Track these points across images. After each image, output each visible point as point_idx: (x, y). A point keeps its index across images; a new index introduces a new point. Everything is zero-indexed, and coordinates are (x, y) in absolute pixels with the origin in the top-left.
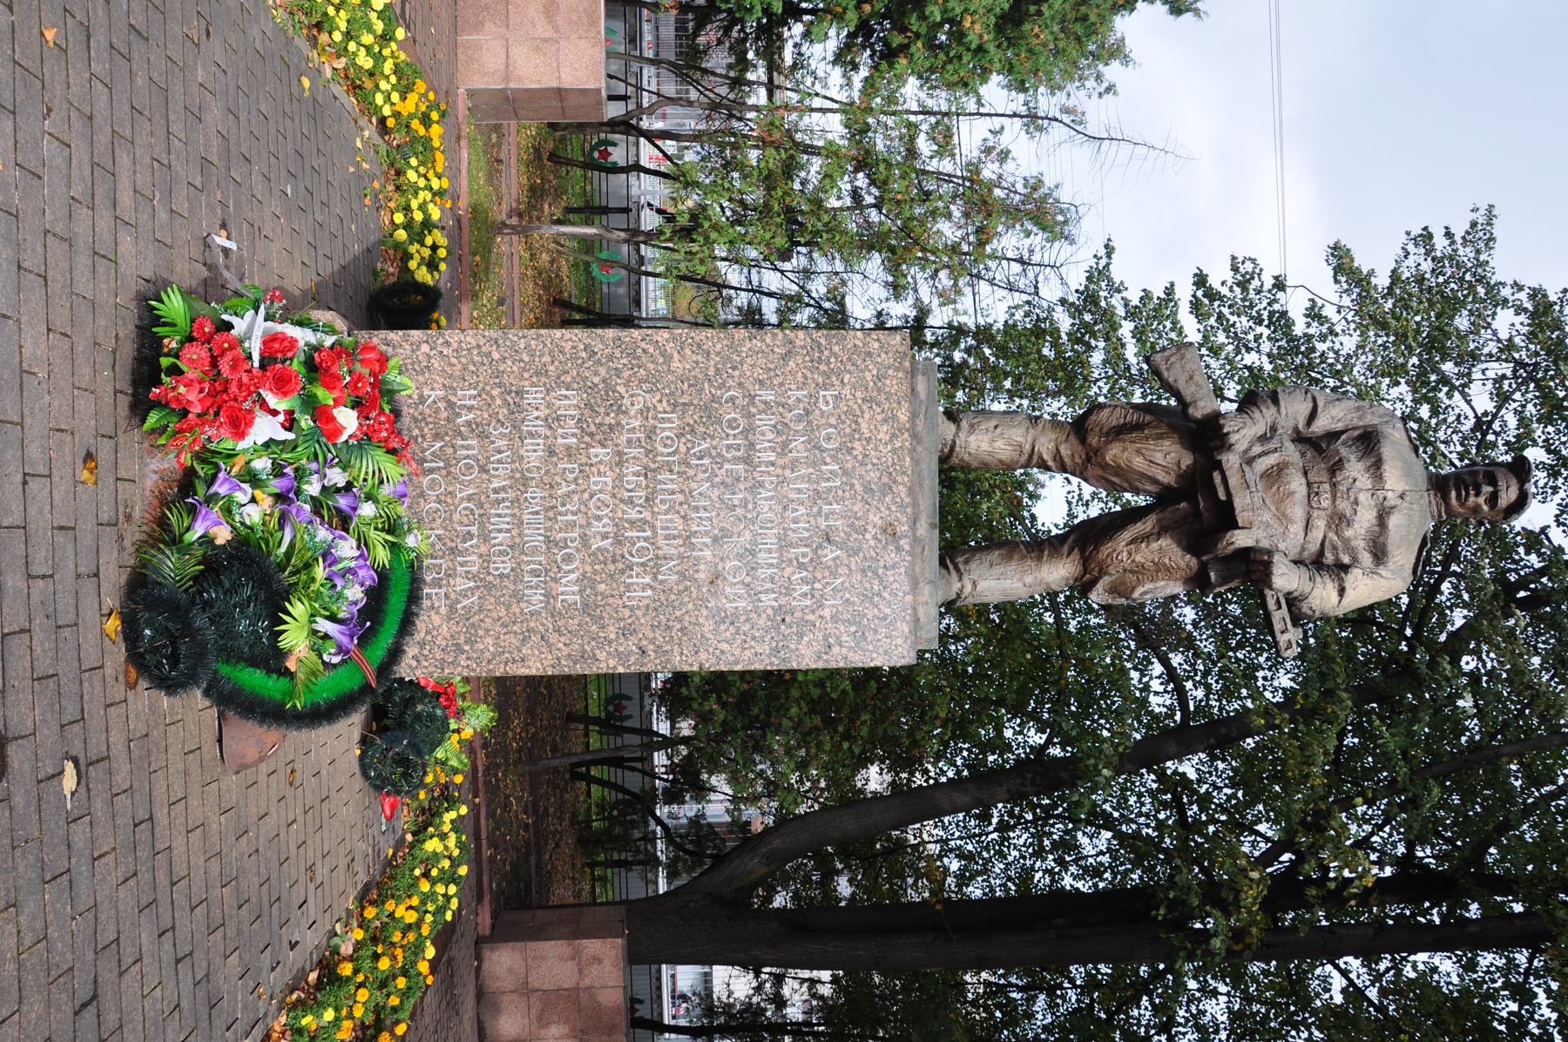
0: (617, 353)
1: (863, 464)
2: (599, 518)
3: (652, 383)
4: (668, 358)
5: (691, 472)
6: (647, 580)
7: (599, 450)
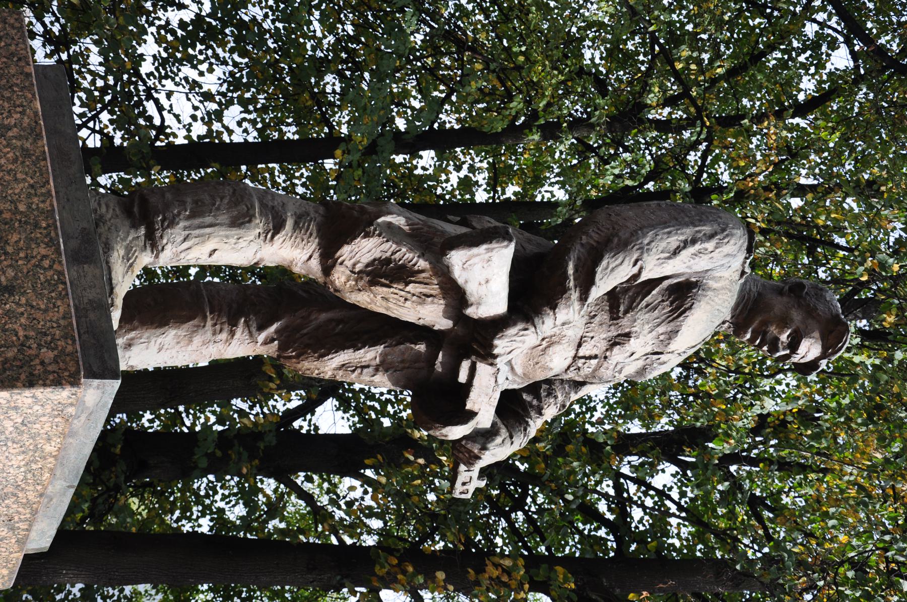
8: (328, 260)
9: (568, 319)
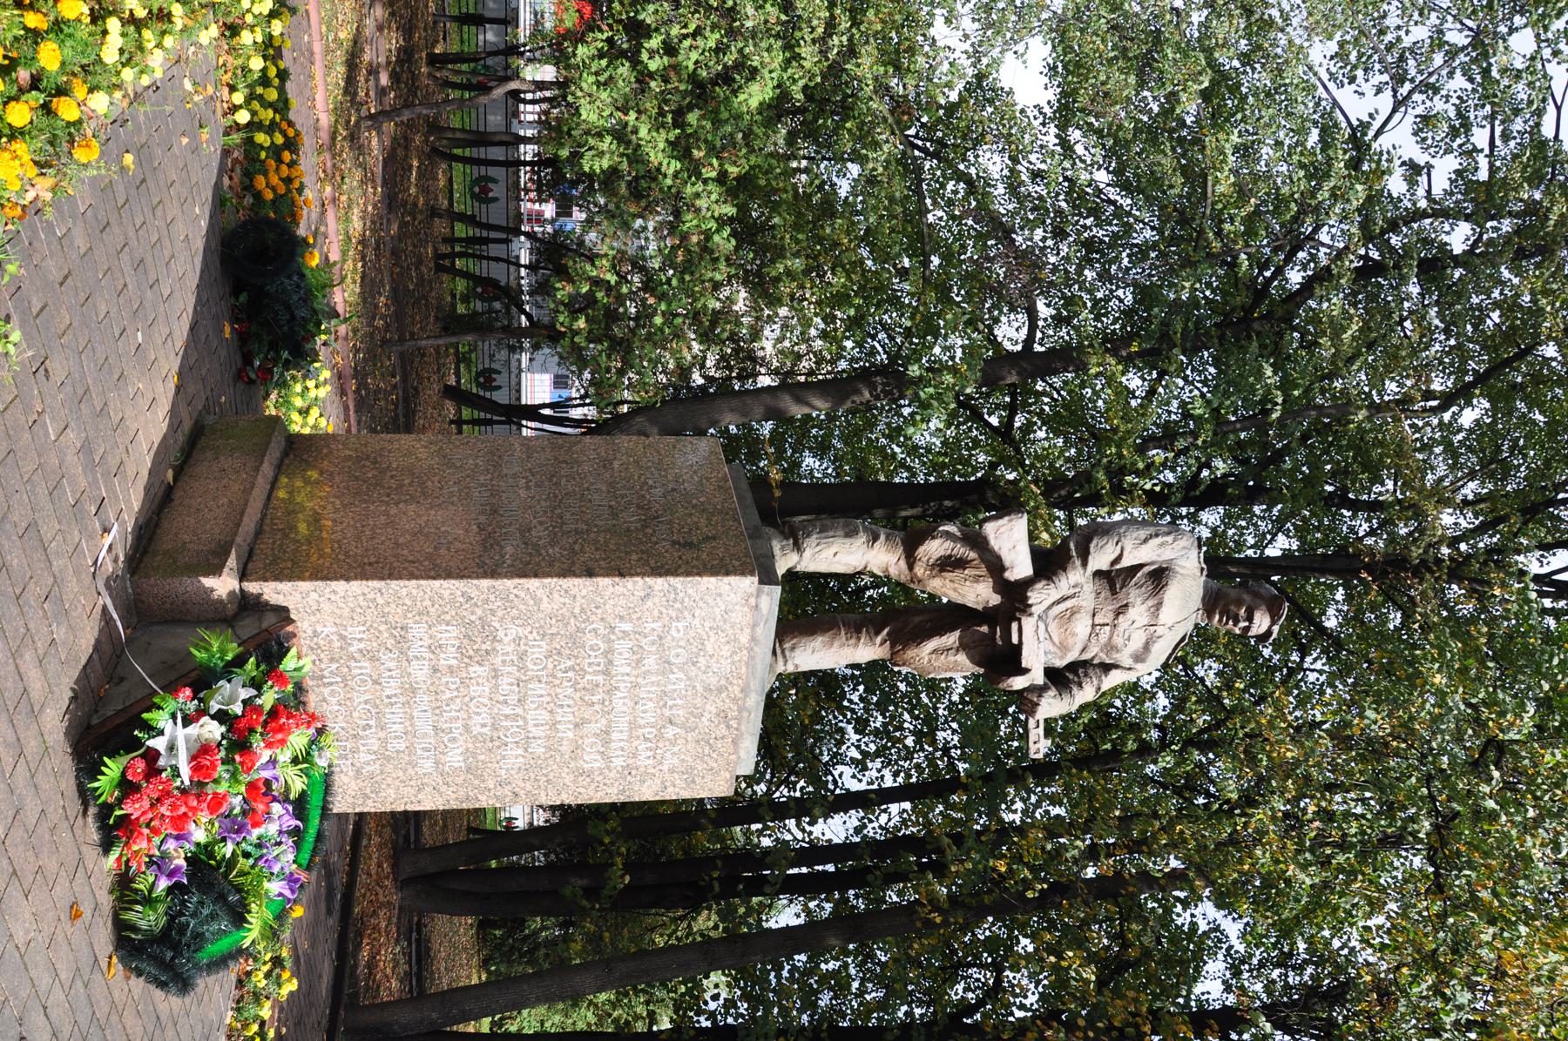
0: (492, 598)
2: (478, 714)
4: (538, 602)
5: (557, 682)
6: (520, 751)
7: (477, 668)
8: (911, 561)
9: (1076, 578)
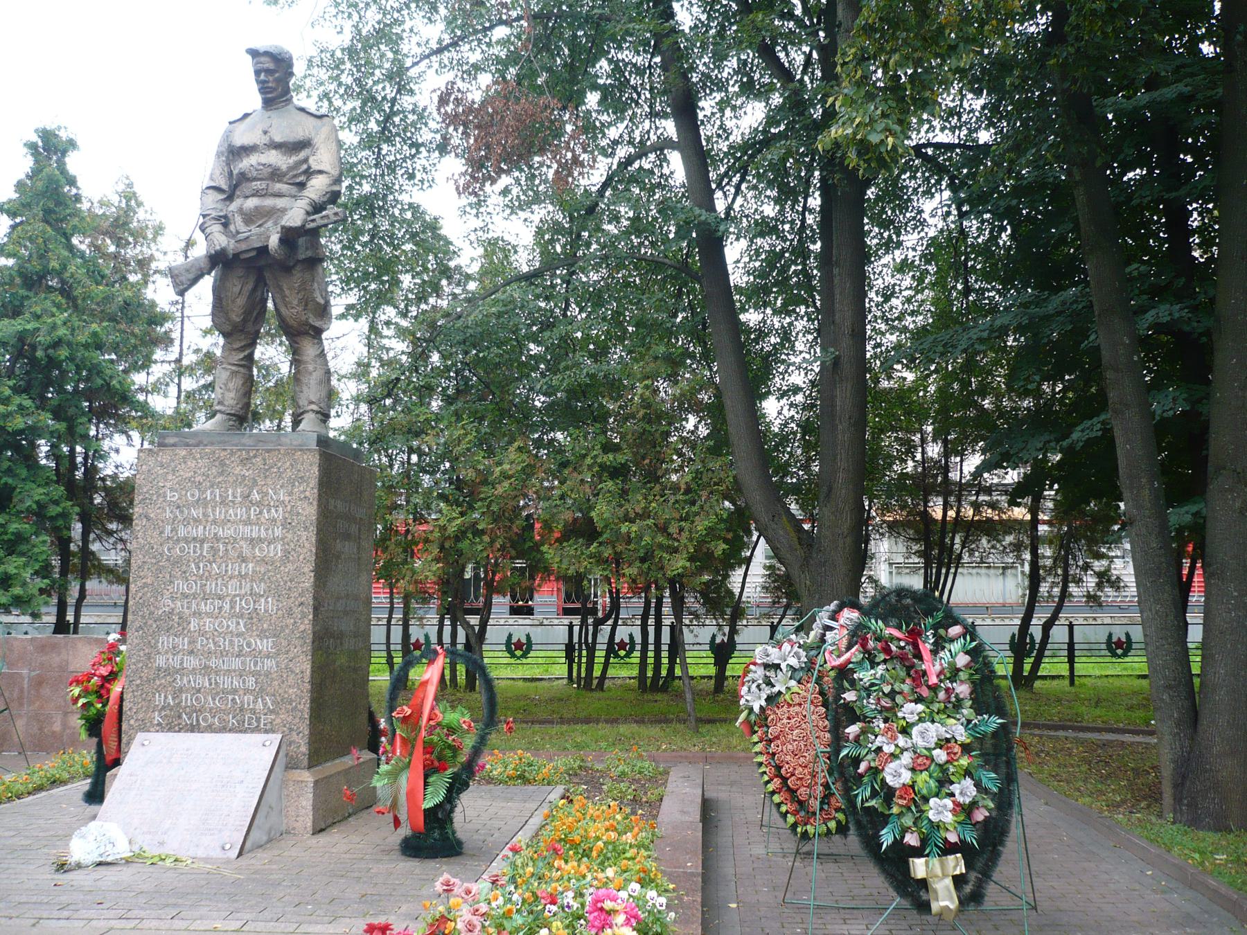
1: (208, 476)
2: (228, 626)
3: (157, 593)
7: (192, 625)
